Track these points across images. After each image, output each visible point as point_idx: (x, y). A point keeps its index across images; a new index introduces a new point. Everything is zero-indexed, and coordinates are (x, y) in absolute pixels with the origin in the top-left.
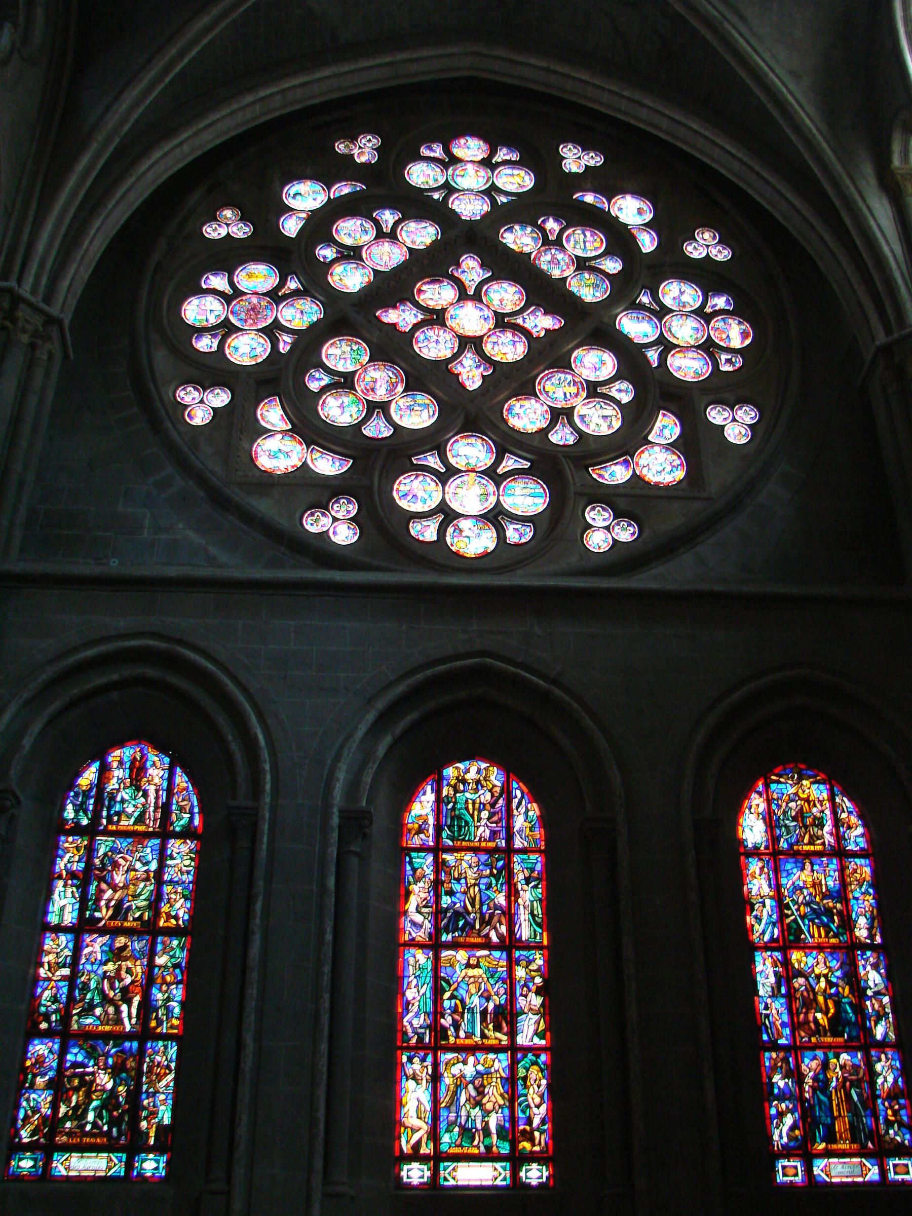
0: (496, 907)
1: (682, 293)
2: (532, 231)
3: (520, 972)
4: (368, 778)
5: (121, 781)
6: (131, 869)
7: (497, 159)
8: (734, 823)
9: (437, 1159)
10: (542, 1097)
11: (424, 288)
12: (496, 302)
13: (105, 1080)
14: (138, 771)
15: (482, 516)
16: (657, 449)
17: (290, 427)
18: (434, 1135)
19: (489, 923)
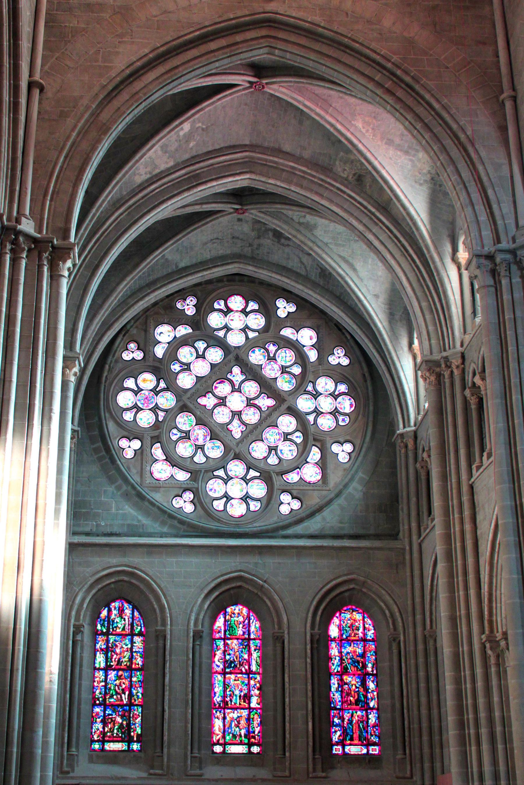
0: (245, 659)
1: (326, 384)
2: (263, 352)
3: (252, 682)
4: (201, 617)
5: (116, 615)
6: (122, 647)
7: (248, 309)
8: (327, 629)
9: (224, 744)
10: (258, 724)
11: (217, 385)
12: (247, 393)
13: (119, 720)
14: (121, 611)
15: (241, 499)
16: (310, 465)
17: (165, 458)
18: (224, 737)
19: (242, 665)
